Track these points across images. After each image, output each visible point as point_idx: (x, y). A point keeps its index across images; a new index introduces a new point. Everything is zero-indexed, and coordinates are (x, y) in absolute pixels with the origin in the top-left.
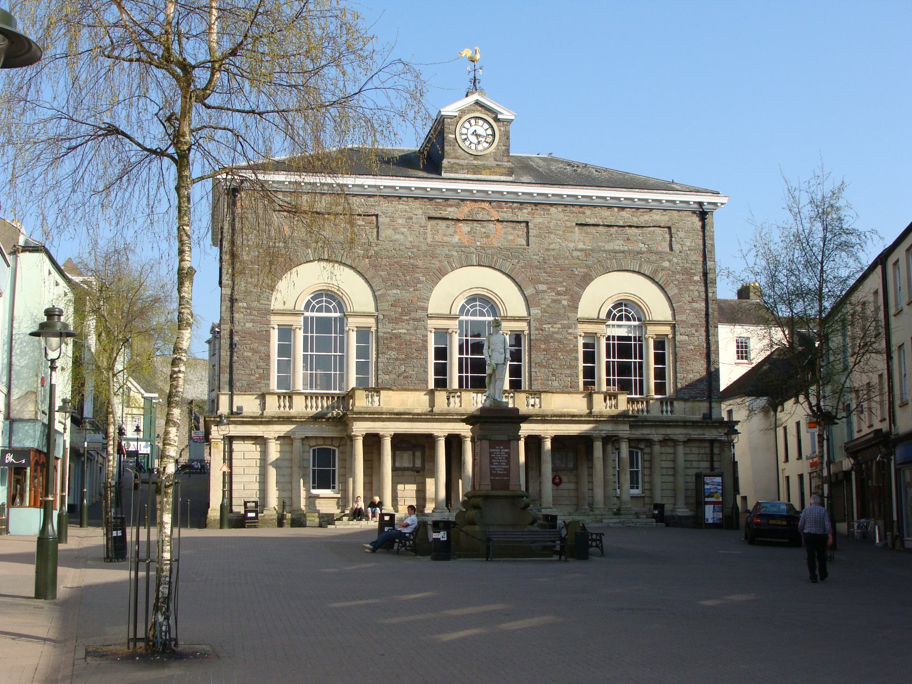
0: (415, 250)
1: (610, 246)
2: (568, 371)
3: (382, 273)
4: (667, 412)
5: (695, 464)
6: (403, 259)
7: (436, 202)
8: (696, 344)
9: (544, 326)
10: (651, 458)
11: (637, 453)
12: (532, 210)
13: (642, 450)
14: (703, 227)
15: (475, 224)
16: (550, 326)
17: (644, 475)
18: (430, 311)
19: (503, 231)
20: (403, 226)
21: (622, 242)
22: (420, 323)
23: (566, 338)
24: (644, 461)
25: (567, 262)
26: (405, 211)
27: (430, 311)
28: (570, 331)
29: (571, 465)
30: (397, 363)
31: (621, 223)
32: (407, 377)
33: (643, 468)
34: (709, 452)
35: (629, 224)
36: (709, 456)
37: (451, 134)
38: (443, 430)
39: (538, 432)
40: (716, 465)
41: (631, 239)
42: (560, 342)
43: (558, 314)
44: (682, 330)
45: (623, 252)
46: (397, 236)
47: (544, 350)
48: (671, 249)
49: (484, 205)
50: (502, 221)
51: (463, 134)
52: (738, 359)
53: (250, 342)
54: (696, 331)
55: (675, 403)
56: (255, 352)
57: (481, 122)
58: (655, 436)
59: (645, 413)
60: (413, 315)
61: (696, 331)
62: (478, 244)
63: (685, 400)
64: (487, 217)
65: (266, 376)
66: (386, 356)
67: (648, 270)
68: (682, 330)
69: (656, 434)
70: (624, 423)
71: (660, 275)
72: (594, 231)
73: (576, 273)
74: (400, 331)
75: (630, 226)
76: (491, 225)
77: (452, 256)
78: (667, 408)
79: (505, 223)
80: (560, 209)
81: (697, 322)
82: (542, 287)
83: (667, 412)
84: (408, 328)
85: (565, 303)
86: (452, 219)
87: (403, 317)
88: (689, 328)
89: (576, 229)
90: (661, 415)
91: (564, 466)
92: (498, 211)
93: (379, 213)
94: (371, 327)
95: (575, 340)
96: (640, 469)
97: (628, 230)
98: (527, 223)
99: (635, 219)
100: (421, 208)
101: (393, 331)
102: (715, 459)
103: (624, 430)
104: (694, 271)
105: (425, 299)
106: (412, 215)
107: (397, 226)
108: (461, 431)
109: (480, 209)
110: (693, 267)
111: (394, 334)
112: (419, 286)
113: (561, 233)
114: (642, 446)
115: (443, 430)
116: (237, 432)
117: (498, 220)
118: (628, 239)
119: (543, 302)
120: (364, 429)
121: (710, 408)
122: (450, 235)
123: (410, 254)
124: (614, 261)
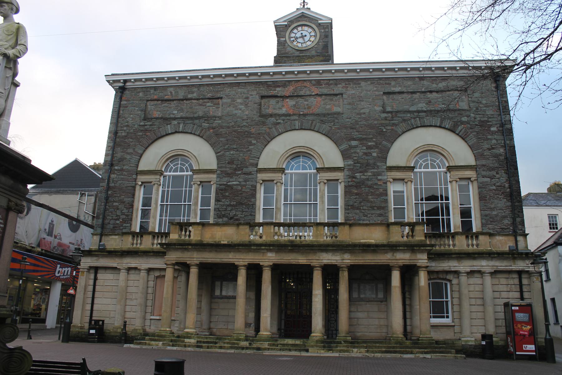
0: (249, 121)
1: (412, 109)
2: (378, 212)
3: (221, 139)
4: (473, 245)
5: (504, 295)
6: (240, 128)
7: (267, 84)
8: (498, 184)
9: (356, 175)
10: (459, 288)
11: (446, 285)
12: (346, 84)
13: (450, 281)
14: (497, 87)
15: (299, 99)
16: (361, 174)
17: (453, 305)
18: (260, 166)
19: (322, 102)
20: (241, 104)
21: (424, 104)
22: (250, 177)
23: (376, 184)
24: (452, 291)
25: (376, 122)
26: (244, 93)
27: (260, 166)
28: (379, 177)
29: (381, 295)
30: (229, 208)
31: (423, 90)
32: (237, 220)
33: (452, 298)
34: (518, 283)
35: (429, 90)
36: (518, 286)
37: (283, 38)
38: (244, 260)
39: (335, 261)
40: (526, 295)
41: (432, 101)
42: (370, 187)
43: (368, 165)
44: (484, 173)
45: (425, 112)
46: (236, 112)
47: (357, 194)
48: (470, 107)
49: (305, 84)
50: (321, 95)
51: (292, 37)
52: (550, 228)
53: (118, 195)
54: (497, 173)
55: (481, 238)
56: (122, 202)
57: (306, 28)
58: (462, 268)
59: (451, 247)
60: (245, 170)
61: (497, 173)
62: (301, 113)
63: (491, 235)
64: (308, 93)
65: (129, 219)
66: (221, 203)
67: (448, 125)
68: (484, 173)
69: (465, 266)
70: (422, 252)
71: (460, 128)
72: (400, 97)
73: (384, 130)
74: (233, 183)
75: (431, 92)
76: (312, 99)
77: (279, 123)
78: (472, 242)
79: (323, 97)
80: (369, 82)
81: (496, 165)
82: (354, 143)
83: (473, 245)
84: (241, 180)
85: (375, 154)
86: (281, 97)
87: (237, 172)
88: (490, 171)
89: (385, 97)
90: (467, 248)
91: (374, 296)
92: (317, 88)
93: (224, 96)
94: (210, 182)
95: (384, 185)
96: (449, 299)
97: (429, 95)
98: (342, 94)
99: (434, 85)
100: (256, 90)
101: (228, 184)
102: (525, 289)
103: (422, 259)
104: (491, 123)
105: (255, 157)
106: (249, 96)
107: (236, 104)
108: (261, 260)
109: (303, 87)
110: (490, 120)
111: (229, 186)
112: (252, 147)
113: (371, 100)
114: (450, 277)
115: (244, 260)
116: (99, 264)
117: (317, 95)
118: (430, 102)
119: (354, 155)
120: (175, 259)
121: (516, 241)
122: (279, 108)
123: (245, 124)
124: (418, 119)
